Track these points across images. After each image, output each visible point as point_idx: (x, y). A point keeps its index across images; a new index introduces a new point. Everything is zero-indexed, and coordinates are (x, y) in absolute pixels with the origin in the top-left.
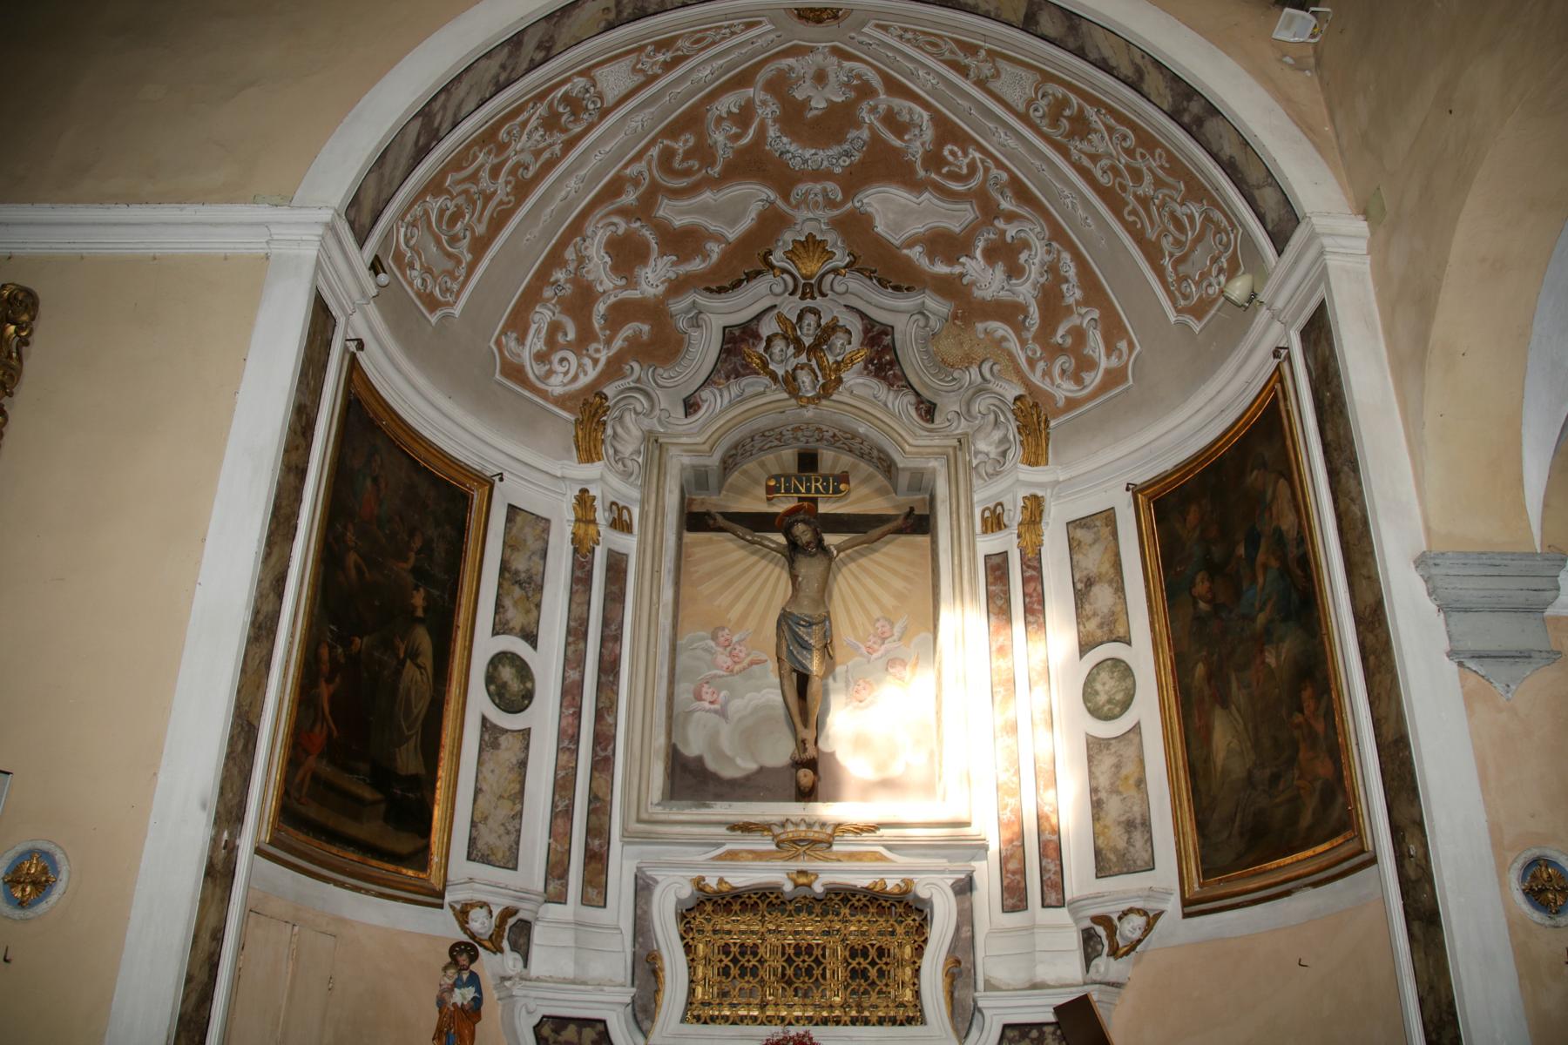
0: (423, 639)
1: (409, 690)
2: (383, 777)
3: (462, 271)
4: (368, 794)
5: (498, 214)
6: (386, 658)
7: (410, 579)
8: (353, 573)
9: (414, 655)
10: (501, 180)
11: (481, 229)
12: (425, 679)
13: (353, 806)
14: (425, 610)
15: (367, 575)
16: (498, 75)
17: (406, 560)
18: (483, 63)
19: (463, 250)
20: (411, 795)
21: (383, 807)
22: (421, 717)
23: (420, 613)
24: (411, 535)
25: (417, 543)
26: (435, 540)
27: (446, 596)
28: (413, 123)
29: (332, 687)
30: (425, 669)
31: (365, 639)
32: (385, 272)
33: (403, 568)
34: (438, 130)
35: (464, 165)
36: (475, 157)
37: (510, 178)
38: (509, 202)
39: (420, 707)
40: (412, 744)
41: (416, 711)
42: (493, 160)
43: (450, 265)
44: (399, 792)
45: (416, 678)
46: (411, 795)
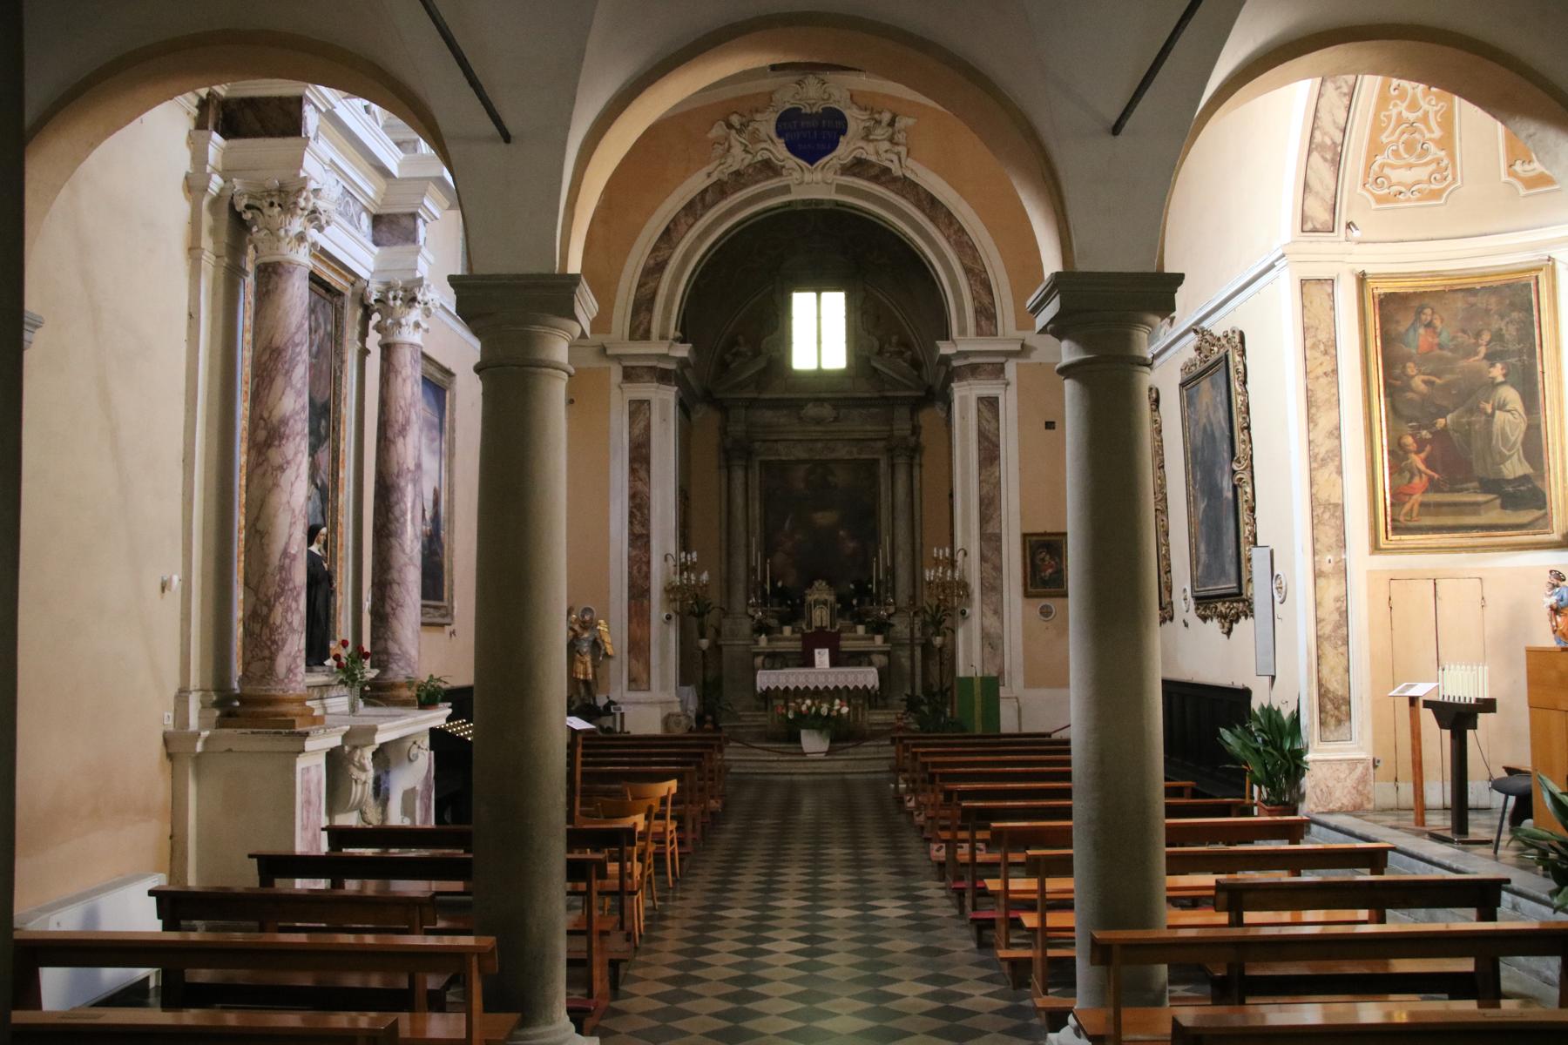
0: (1510, 395)
1: (1503, 429)
2: (1494, 485)
3: (1446, 162)
4: (1481, 498)
5: (1441, 117)
6: (1473, 419)
7: (1485, 364)
8: (1422, 387)
9: (1502, 407)
10: (1422, 103)
11: (1437, 133)
12: (1517, 416)
13: (1475, 507)
14: (1505, 375)
15: (1438, 381)
16: (1341, 93)
17: (1476, 354)
18: (1322, 101)
19: (1435, 151)
20: (1522, 488)
21: (1498, 502)
22: (1520, 440)
23: (1500, 379)
24: (1478, 335)
25: (1486, 337)
26: (1504, 328)
27: (1525, 358)
28: (1311, 159)
29: (1423, 455)
30: (1516, 410)
31: (1449, 417)
32: (1357, 229)
33: (1477, 361)
34: (1334, 143)
35: (1383, 125)
36: (1389, 117)
37: (1428, 99)
38: (1442, 107)
39: (1517, 433)
40: (1516, 456)
41: (1513, 439)
42: (1403, 107)
43: (1433, 166)
44: (1511, 489)
45: (1510, 420)
46: (1522, 488)
